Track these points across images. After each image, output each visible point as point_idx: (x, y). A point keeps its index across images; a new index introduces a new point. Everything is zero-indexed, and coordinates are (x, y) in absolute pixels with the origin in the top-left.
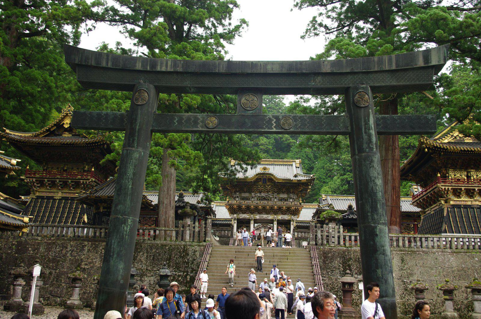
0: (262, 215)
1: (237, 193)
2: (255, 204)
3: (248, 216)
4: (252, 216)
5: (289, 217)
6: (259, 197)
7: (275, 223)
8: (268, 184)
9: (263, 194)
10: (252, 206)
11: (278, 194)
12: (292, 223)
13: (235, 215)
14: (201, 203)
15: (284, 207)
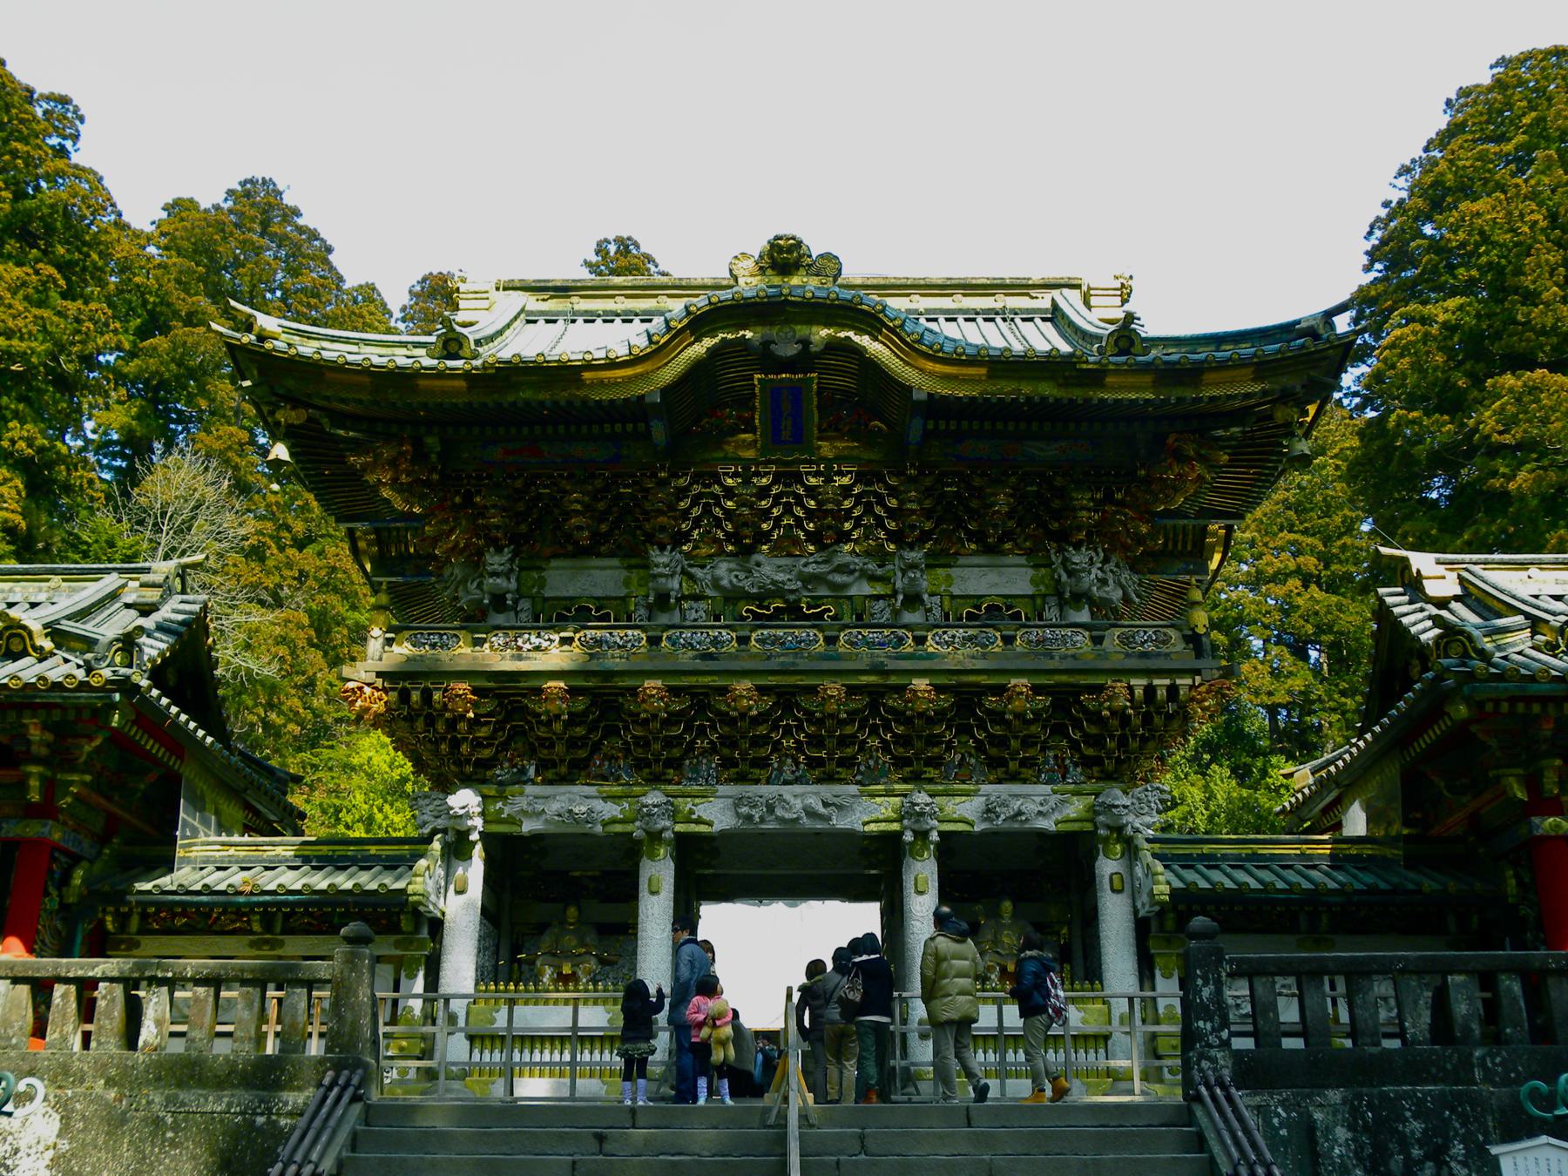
0: (767, 790)
1: (495, 561)
2: (685, 659)
3: (610, 810)
4: (654, 798)
5: (1076, 807)
6: (733, 596)
7: (923, 873)
8: (826, 449)
9: (770, 569)
10: (652, 685)
11: (940, 559)
12: (1108, 866)
13: (465, 800)
14: (43, 656)
15: (1021, 683)
